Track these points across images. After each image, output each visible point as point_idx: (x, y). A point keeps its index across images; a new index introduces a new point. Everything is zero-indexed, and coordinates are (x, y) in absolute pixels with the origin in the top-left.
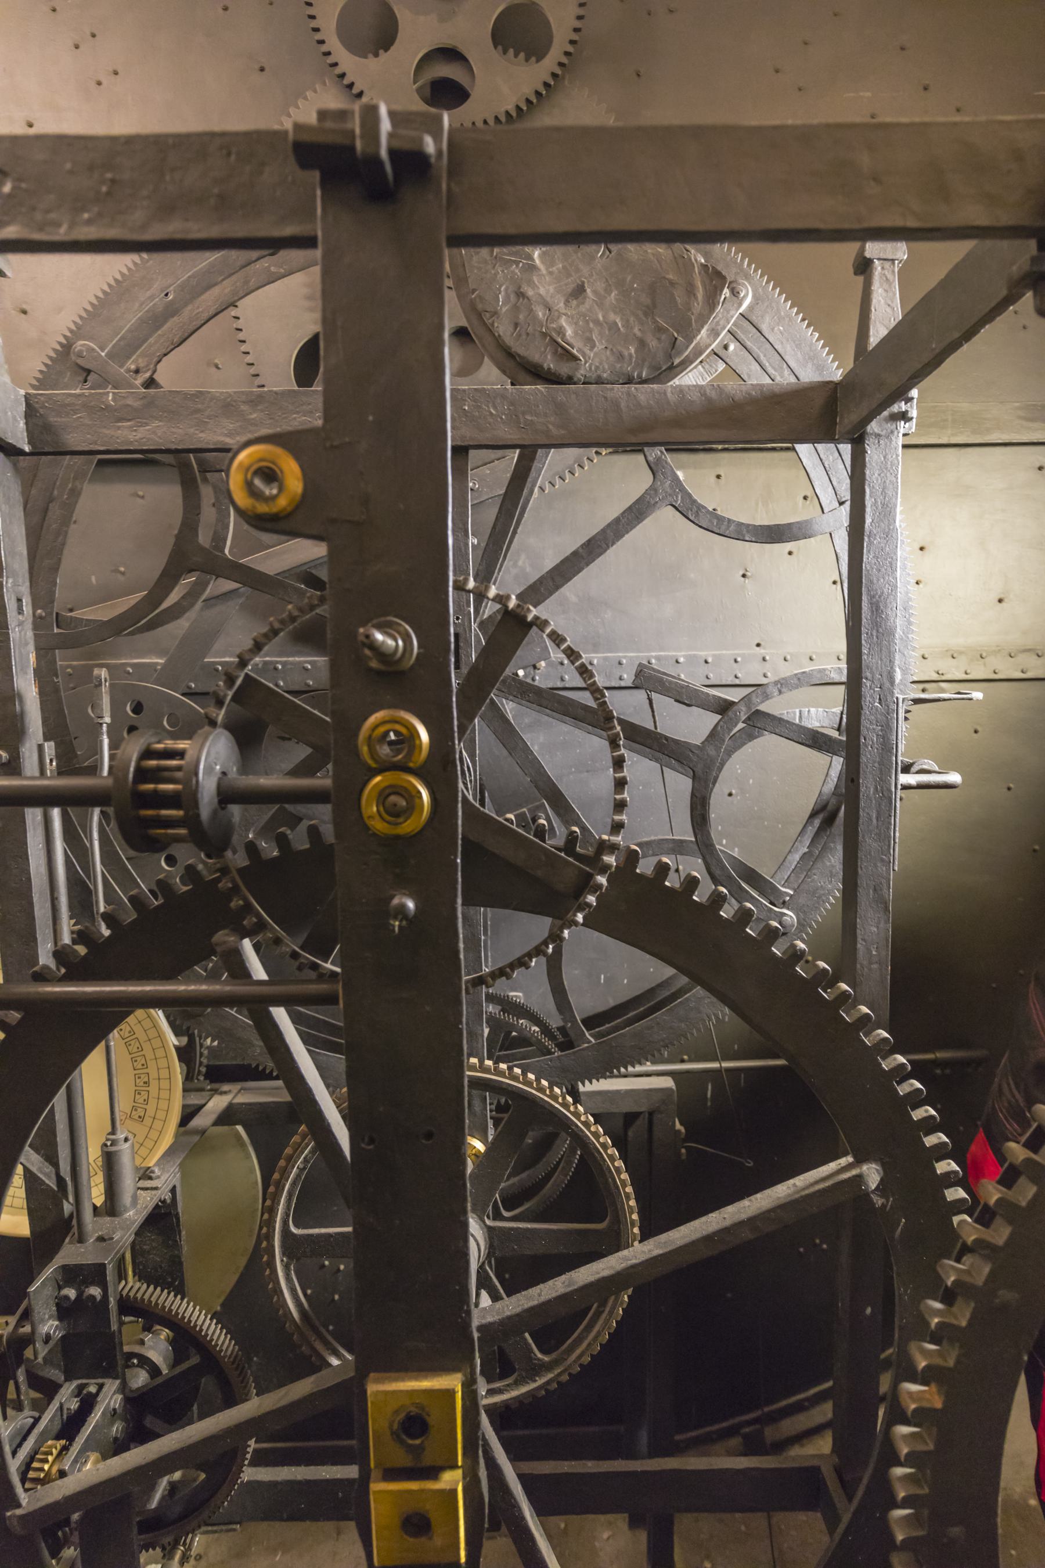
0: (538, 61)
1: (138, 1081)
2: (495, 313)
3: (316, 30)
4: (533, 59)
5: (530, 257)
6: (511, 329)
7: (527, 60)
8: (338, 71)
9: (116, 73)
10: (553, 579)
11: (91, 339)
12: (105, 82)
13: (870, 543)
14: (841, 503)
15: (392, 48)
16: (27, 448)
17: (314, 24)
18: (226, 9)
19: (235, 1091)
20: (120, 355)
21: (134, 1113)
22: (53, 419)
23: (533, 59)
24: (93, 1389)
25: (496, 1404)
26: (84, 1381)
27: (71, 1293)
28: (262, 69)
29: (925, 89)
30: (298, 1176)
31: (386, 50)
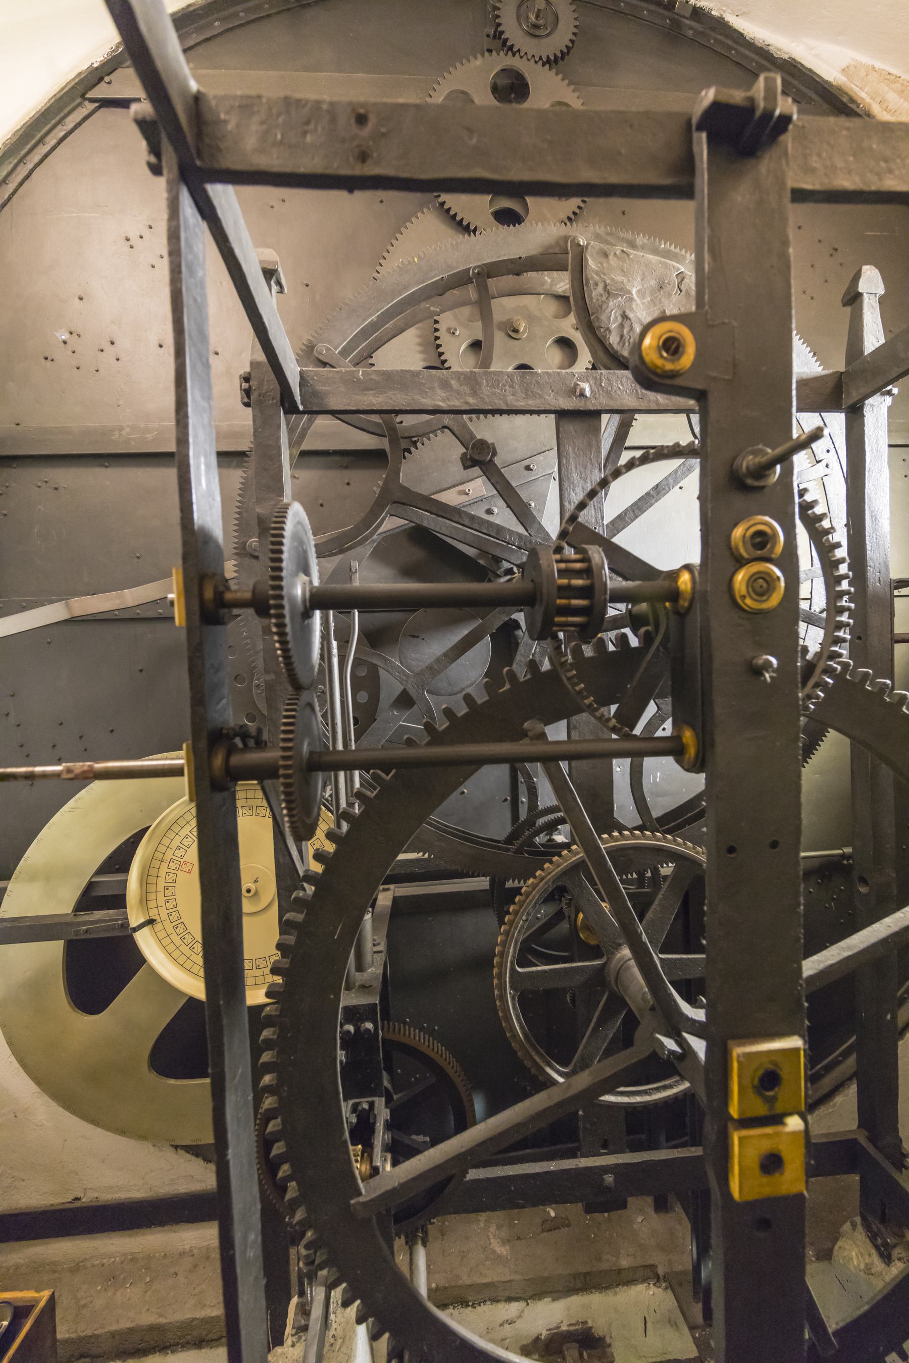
2: (608, 329)
5: (630, 292)
6: (618, 339)
10: (633, 511)
11: (329, 343)
13: (870, 476)
14: (818, 462)
16: (301, 408)
20: (345, 352)
22: (319, 388)
24: (366, 1106)
25: (669, 1096)
26: (357, 1100)
27: (351, 1028)
28: (381, 202)
29: (799, 228)
30: (522, 926)
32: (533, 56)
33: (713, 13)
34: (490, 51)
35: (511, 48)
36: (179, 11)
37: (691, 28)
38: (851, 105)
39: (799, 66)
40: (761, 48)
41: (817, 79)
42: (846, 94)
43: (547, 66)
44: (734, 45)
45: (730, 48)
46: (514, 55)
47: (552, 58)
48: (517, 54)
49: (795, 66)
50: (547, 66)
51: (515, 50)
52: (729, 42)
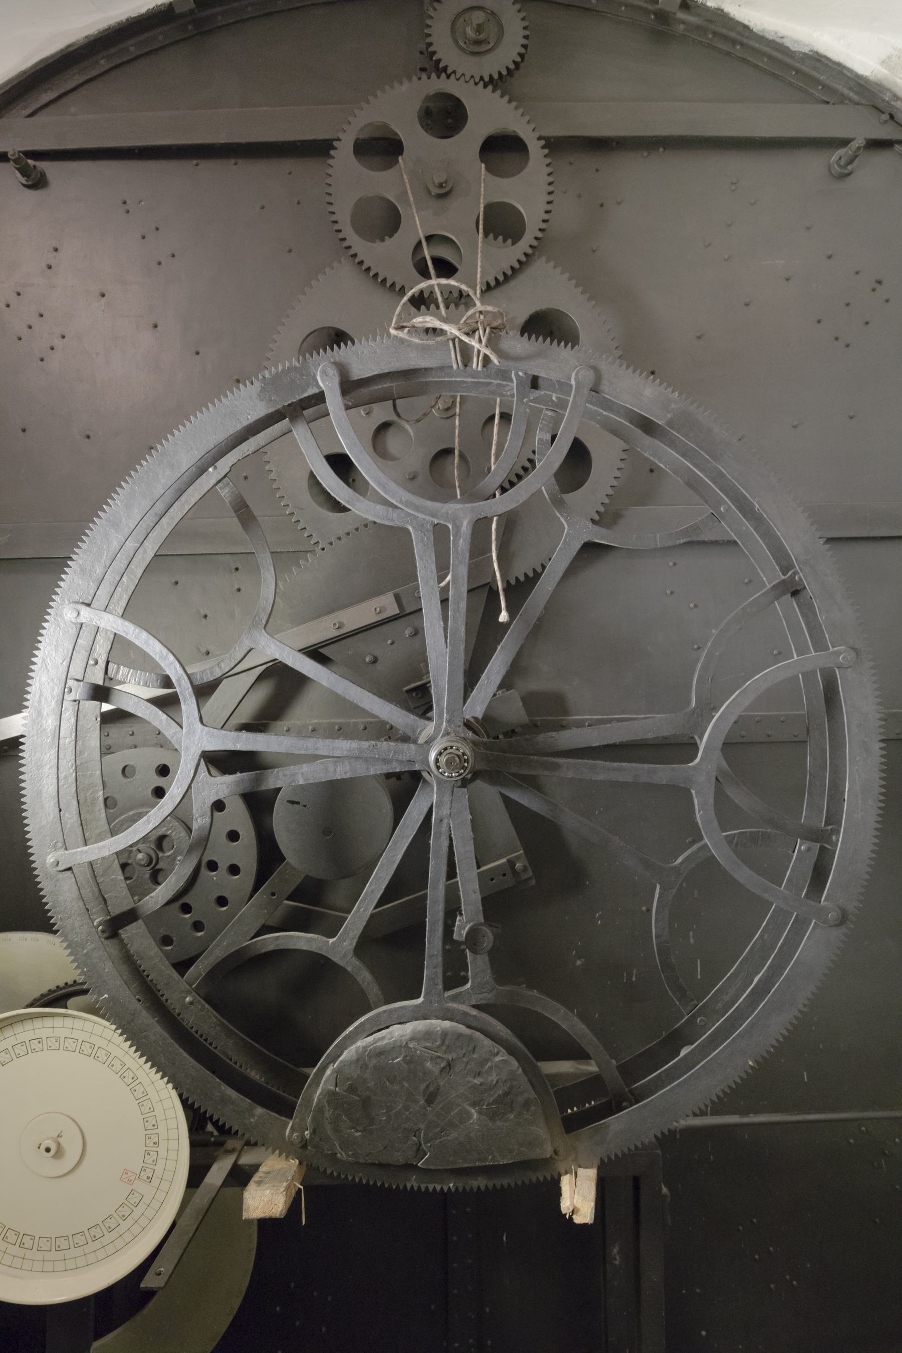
0: (513, 244)
1: (148, 1141)
3: (336, 222)
4: (509, 241)
7: (505, 241)
8: (352, 252)
9: (173, 256)
12: (163, 263)
15: (396, 235)
17: (334, 218)
18: (263, 208)
19: (239, 1147)
21: (143, 1173)
23: (509, 241)
28: (290, 251)
31: (391, 236)
32: (472, 77)
33: (709, 4)
34: (423, 70)
35: (445, 69)
36: (57, 53)
37: (683, 22)
38: (893, 103)
39: (823, 59)
40: (773, 41)
41: (849, 75)
42: (889, 90)
43: (490, 88)
44: (739, 38)
45: (734, 42)
46: (448, 77)
47: (496, 76)
48: (453, 76)
49: (819, 61)
50: (490, 88)
51: (449, 72)
52: (733, 35)
